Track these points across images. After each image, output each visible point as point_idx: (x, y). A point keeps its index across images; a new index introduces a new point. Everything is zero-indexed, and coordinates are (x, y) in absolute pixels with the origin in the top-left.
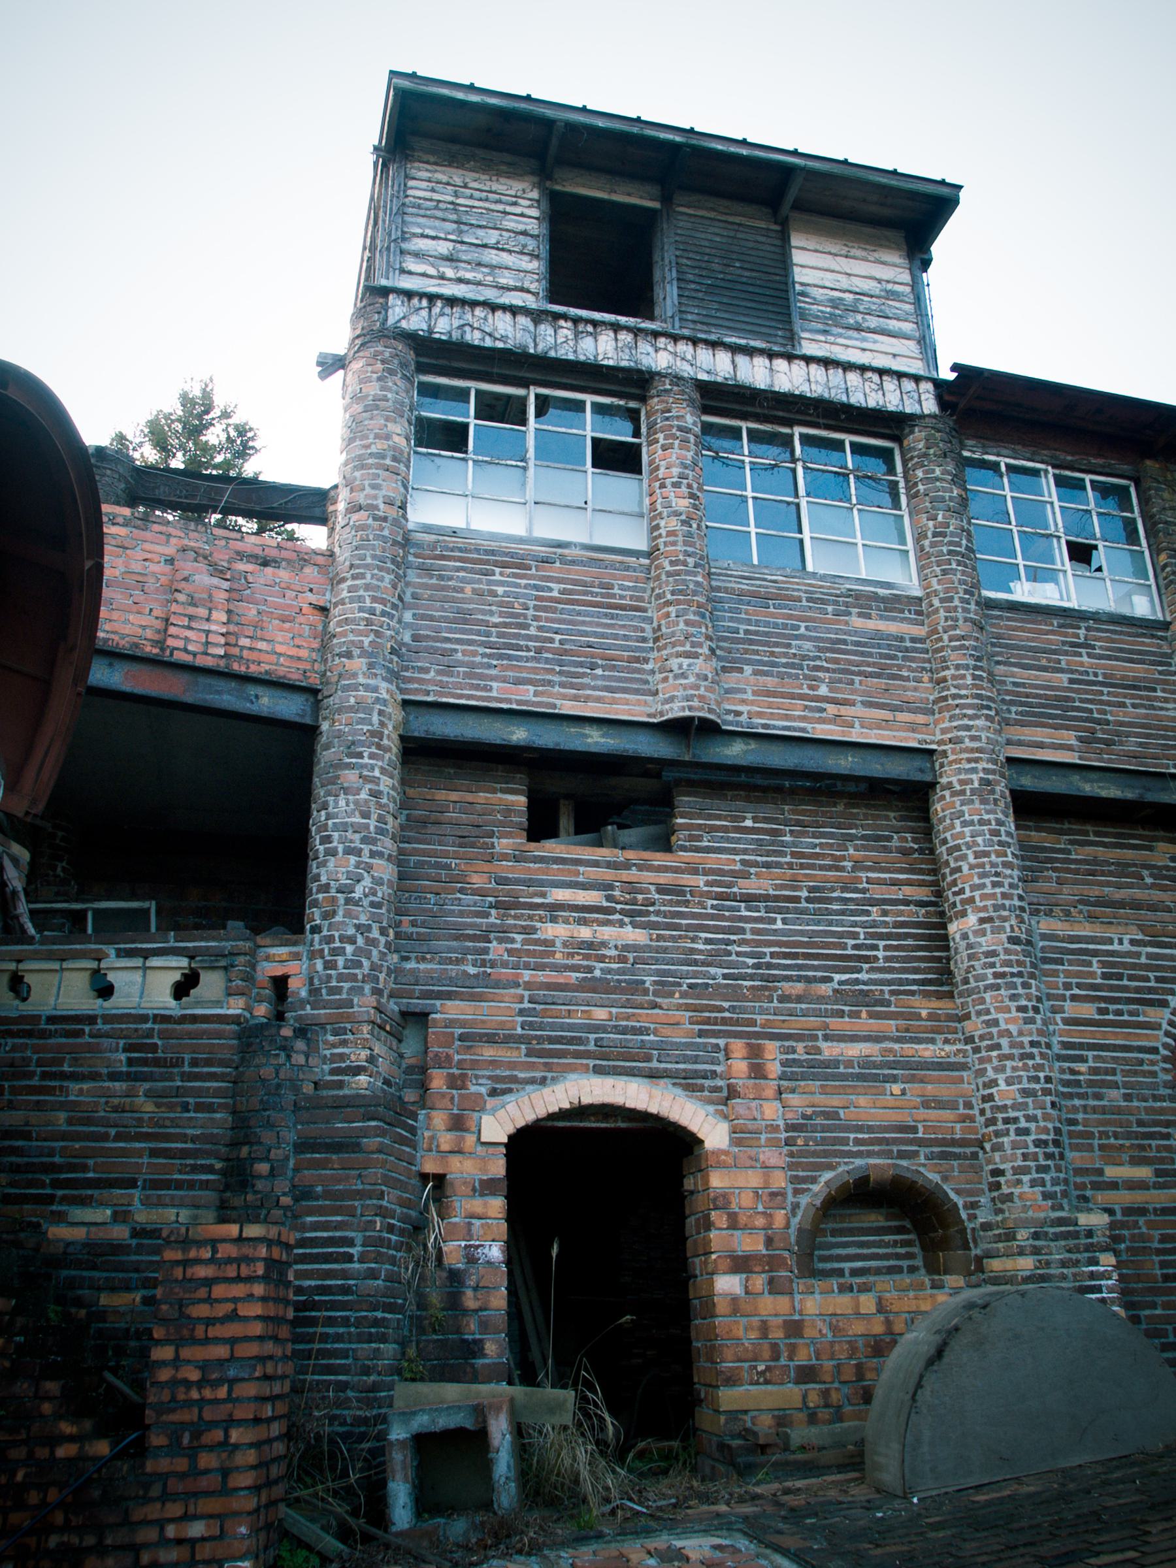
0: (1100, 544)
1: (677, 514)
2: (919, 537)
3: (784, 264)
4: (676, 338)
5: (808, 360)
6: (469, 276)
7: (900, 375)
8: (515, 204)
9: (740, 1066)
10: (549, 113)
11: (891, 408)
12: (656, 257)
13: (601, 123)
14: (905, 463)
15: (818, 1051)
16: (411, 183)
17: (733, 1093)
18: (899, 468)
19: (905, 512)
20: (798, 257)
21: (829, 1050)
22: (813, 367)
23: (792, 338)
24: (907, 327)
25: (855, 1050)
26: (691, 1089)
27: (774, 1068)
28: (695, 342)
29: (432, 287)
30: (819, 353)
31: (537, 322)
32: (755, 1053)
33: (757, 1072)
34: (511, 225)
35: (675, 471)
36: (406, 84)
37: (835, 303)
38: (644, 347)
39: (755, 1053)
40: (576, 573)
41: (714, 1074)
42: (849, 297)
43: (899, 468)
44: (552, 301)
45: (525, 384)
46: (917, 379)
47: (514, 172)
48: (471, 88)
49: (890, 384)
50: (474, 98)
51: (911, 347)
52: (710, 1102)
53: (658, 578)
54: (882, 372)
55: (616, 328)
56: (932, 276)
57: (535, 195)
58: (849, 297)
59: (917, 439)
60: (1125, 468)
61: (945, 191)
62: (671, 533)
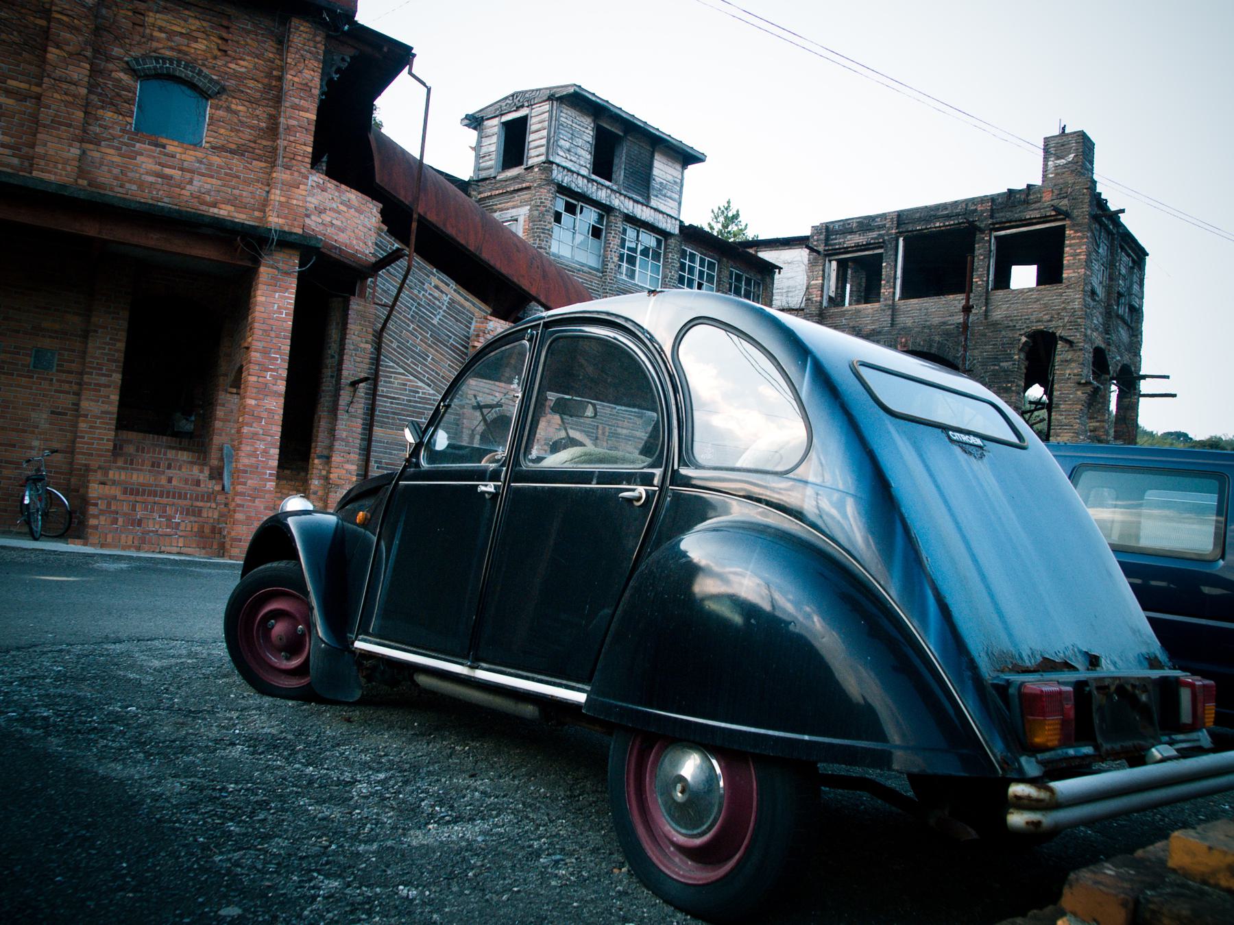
0: (705, 283)
1: (613, 262)
2: (664, 277)
3: (650, 166)
4: (621, 194)
5: (651, 208)
6: (573, 159)
7: (672, 217)
8: (587, 128)
9: (600, 432)
10: (612, 108)
11: (668, 230)
12: (617, 153)
13: (624, 115)
14: (665, 249)
15: (616, 430)
16: (562, 114)
17: (597, 438)
18: (663, 248)
19: (661, 264)
20: (657, 164)
21: (619, 430)
22: (652, 211)
23: (648, 198)
24: (677, 197)
25: (625, 431)
26: (588, 436)
27: (607, 434)
28: (625, 196)
29: (564, 164)
30: (655, 206)
31: (588, 182)
32: (604, 428)
33: (603, 434)
34: (585, 138)
35: (616, 247)
36: (577, 89)
37: (661, 183)
38: (613, 196)
39: (604, 428)
40: (586, 276)
41: (593, 433)
42: (664, 182)
43: (663, 248)
44: (593, 173)
45: (578, 201)
46: (676, 219)
47: (588, 115)
48: (594, 94)
49: (669, 220)
50: (594, 99)
51: (675, 205)
52: (591, 440)
53: (605, 282)
54: (668, 215)
55: (608, 187)
56: (686, 171)
57: (592, 125)
58: (664, 182)
59: (672, 241)
60: (717, 257)
61: (703, 157)
62: (611, 269)
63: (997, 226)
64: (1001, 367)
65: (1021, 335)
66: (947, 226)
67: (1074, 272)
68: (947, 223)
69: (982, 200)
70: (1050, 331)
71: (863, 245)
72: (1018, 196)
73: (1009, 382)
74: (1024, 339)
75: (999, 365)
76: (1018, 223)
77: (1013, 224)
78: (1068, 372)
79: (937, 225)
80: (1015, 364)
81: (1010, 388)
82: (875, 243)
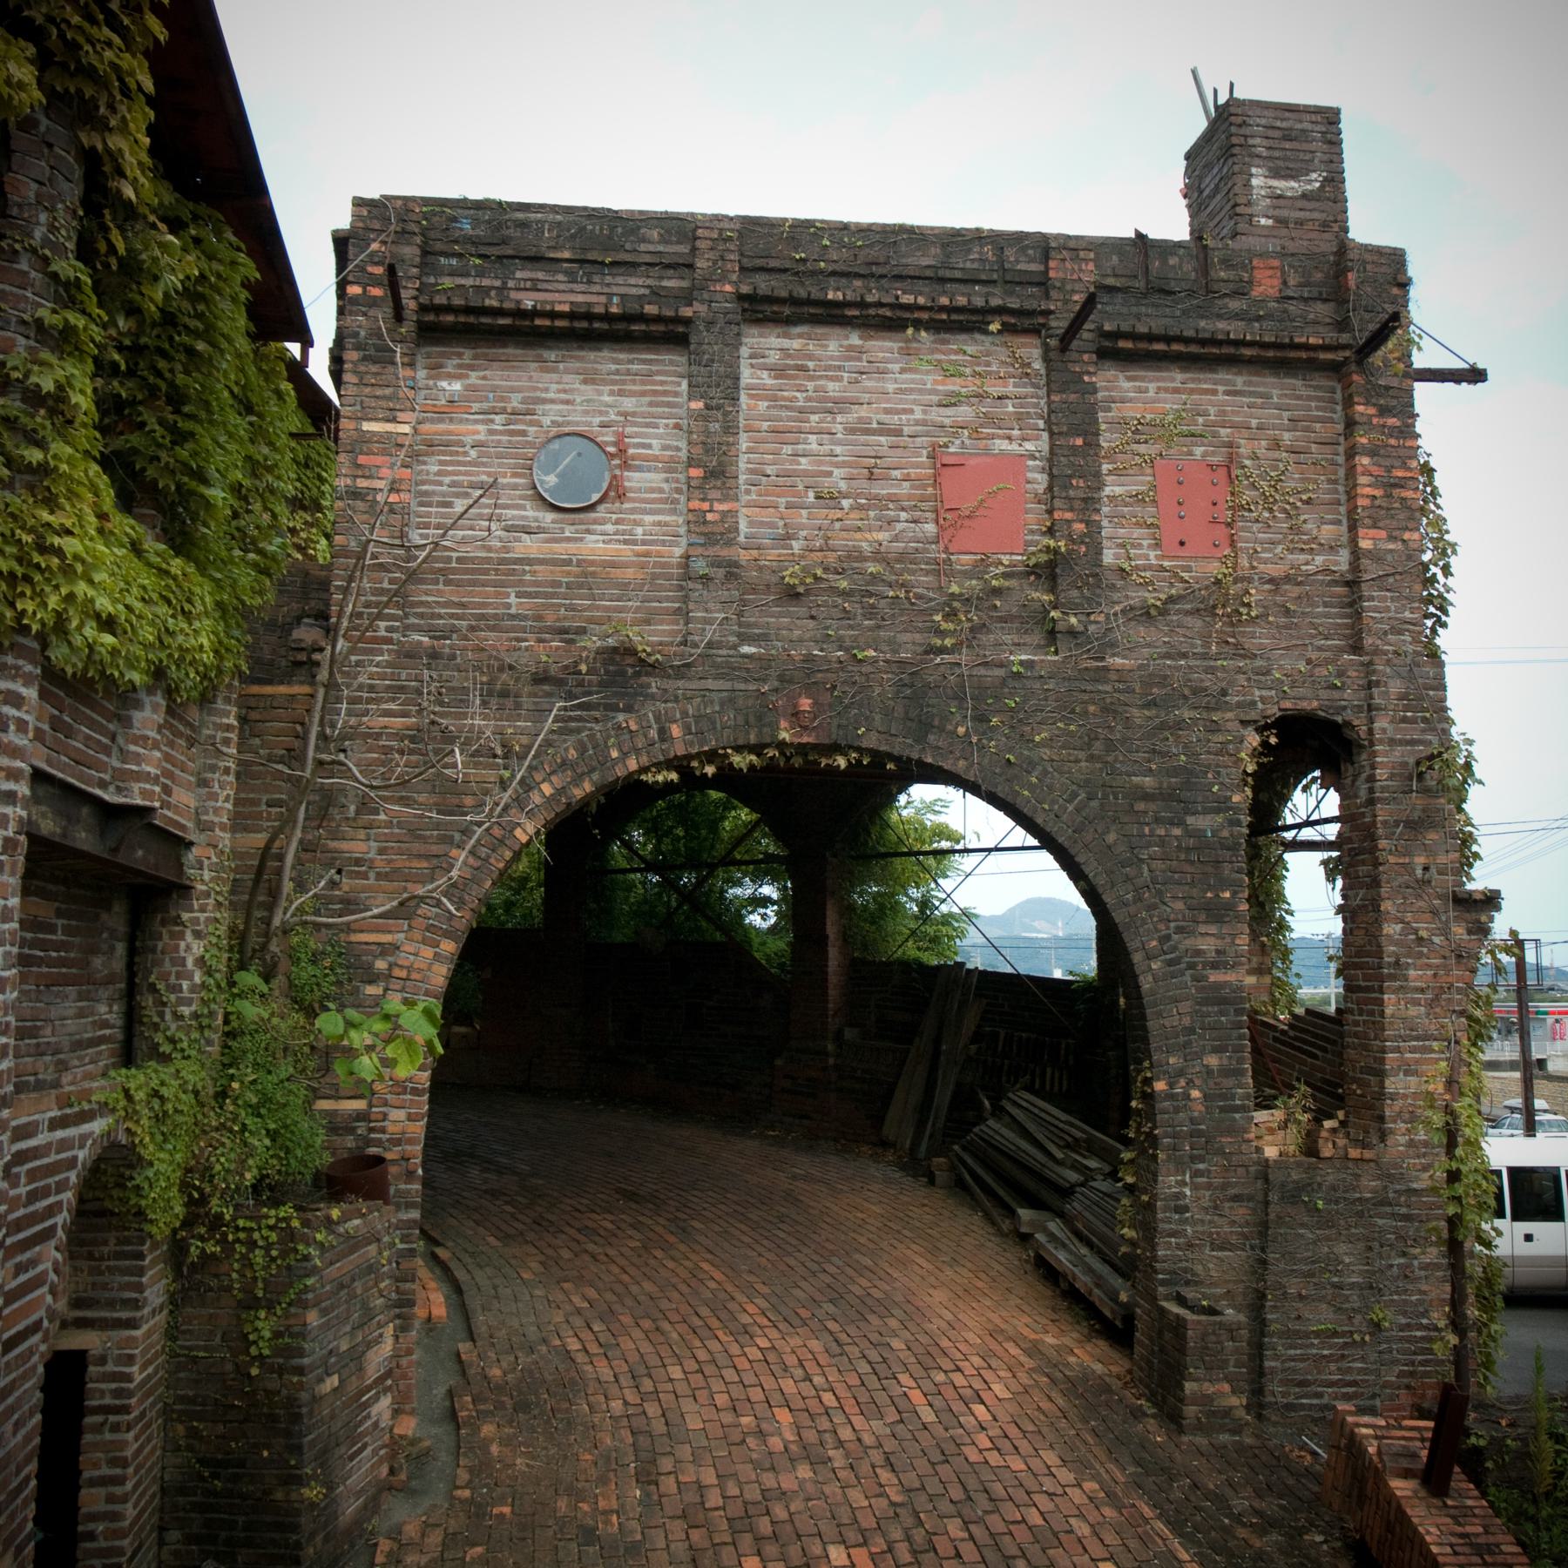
63: (1122, 344)
64: (1189, 833)
65: (1244, 723)
66: (942, 309)
67: (1392, 538)
68: (944, 301)
69: (1073, 247)
70: (1339, 719)
71: (607, 317)
72: (1173, 261)
73: (1223, 884)
74: (1254, 740)
75: (1181, 823)
76: (1193, 349)
77: (1175, 347)
78: (1420, 860)
79: (907, 299)
80: (1238, 822)
81: (1230, 906)
82: (658, 319)
